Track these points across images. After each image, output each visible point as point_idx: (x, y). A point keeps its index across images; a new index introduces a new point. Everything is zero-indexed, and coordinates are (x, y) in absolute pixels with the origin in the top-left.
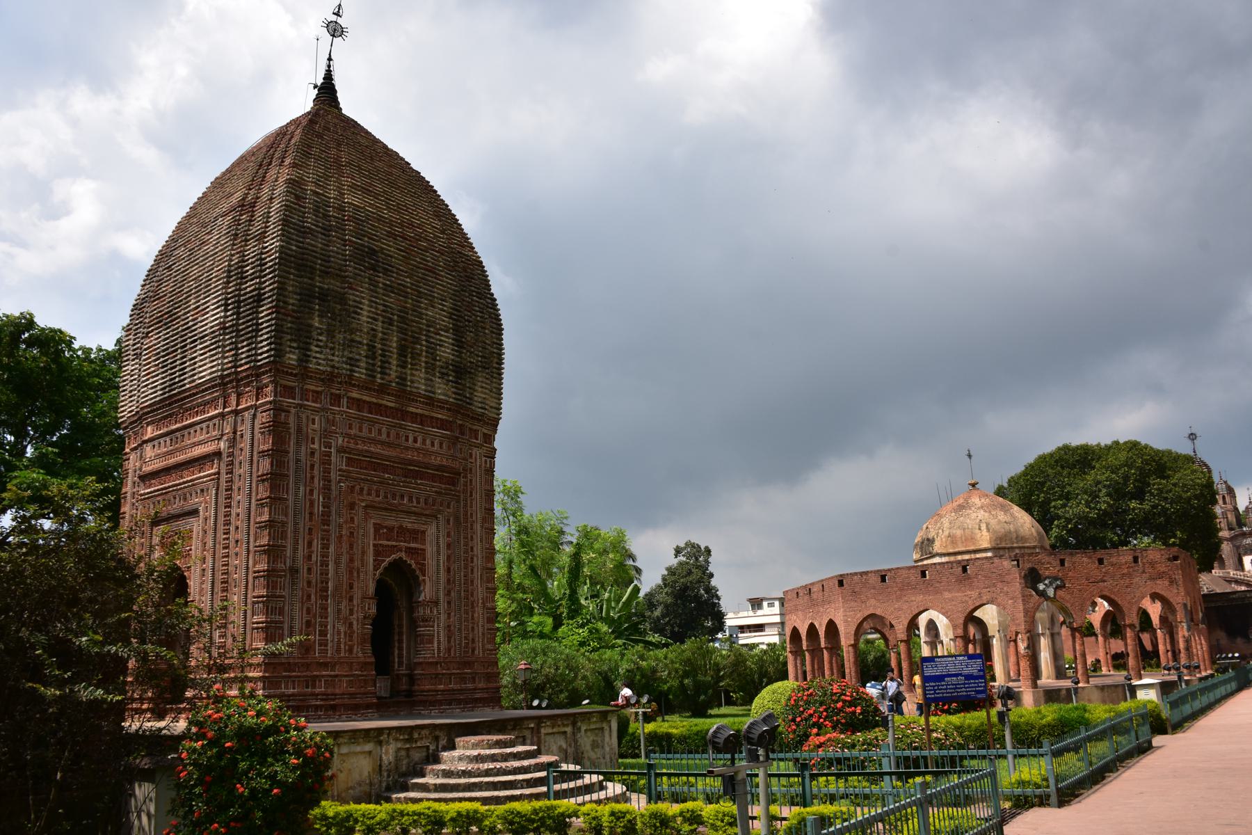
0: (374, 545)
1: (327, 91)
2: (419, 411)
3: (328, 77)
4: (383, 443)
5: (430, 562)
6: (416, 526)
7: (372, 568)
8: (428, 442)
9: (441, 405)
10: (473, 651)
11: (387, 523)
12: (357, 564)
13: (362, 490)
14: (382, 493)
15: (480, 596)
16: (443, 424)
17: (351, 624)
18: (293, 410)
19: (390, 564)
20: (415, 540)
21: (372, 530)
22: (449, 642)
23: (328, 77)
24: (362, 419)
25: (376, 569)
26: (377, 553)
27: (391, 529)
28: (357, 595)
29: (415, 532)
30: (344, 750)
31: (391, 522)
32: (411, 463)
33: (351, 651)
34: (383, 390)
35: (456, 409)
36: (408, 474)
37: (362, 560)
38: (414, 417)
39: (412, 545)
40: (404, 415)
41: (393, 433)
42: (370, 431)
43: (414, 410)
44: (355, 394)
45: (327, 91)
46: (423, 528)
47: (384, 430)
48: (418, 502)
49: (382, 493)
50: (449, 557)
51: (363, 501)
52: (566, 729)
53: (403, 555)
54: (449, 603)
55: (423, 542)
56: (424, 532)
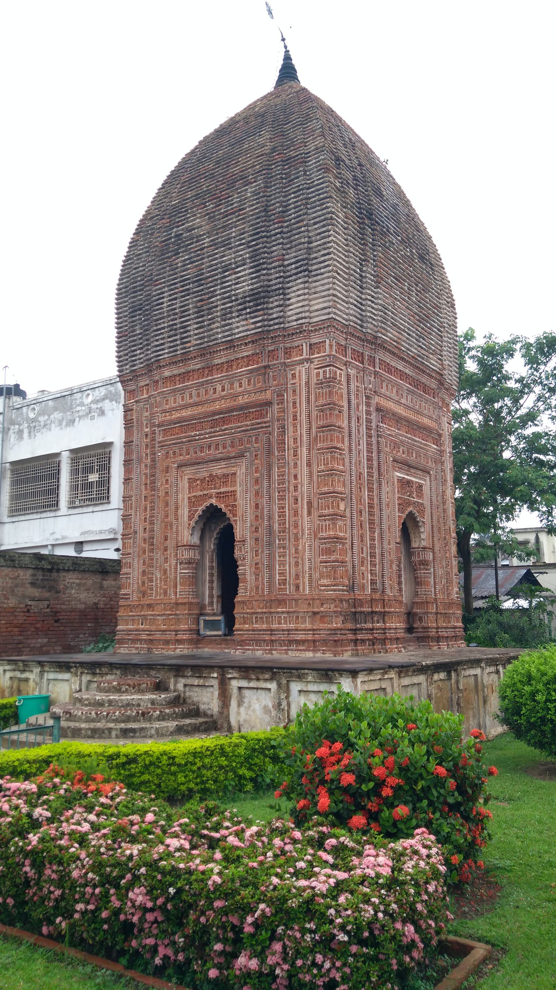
0: (189, 498)
1: (288, 71)
2: (224, 360)
3: (287, 58)
4: (192, 405)
5: (240, 502)
6: (225, 471)
7: (186, 518)
8: (236, 385)
9: (244, 342)
10: (297, 587)
11: (198, 476)
12: (171, 518)
13: (174, 453)
14: (192, 451)
15: (306, 526)
16: (249, 359)
17: (165, 571)
18: (134, 407)
19: (203, 511)
20: (225, 483)
21: (187, 485)
22: (257, 579)
23: (287, 58)
24: (174, 391)
25: (190, 518)
26: (192, 502)
27: (203, 480)
28: (170, 543)
29: (226, 476)
30: (52, 676)
31: (203, 472)
32: (214, 413)
33: (165, 593)
34: (185, 358)
35: (258, 339)
36: (214, 424)
37: (176, 515)
38: (220, 367)
39: (222, 490)
40: (210, 369)
41: (202, 391)
42: (183, 399)
43: (219, 361)
44: (167, 373)
45: (288, 71)
46: (233, 470)
47: (194, 392)
48: (224, 447)
49: (192, 451)
50: (257, 493)
51: (174, 463)
52: (268, 685)
53: (213, 501)
54: (257, 540)
55: (234, 483)
56: (234, 474)
